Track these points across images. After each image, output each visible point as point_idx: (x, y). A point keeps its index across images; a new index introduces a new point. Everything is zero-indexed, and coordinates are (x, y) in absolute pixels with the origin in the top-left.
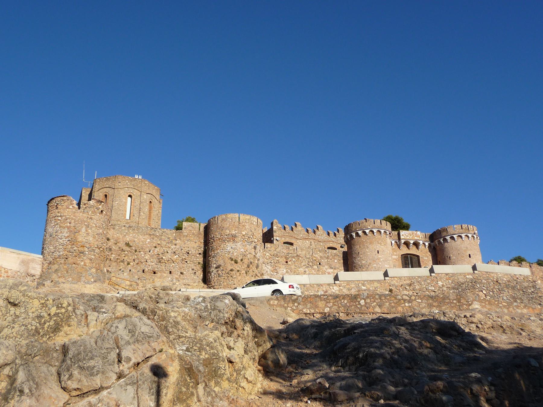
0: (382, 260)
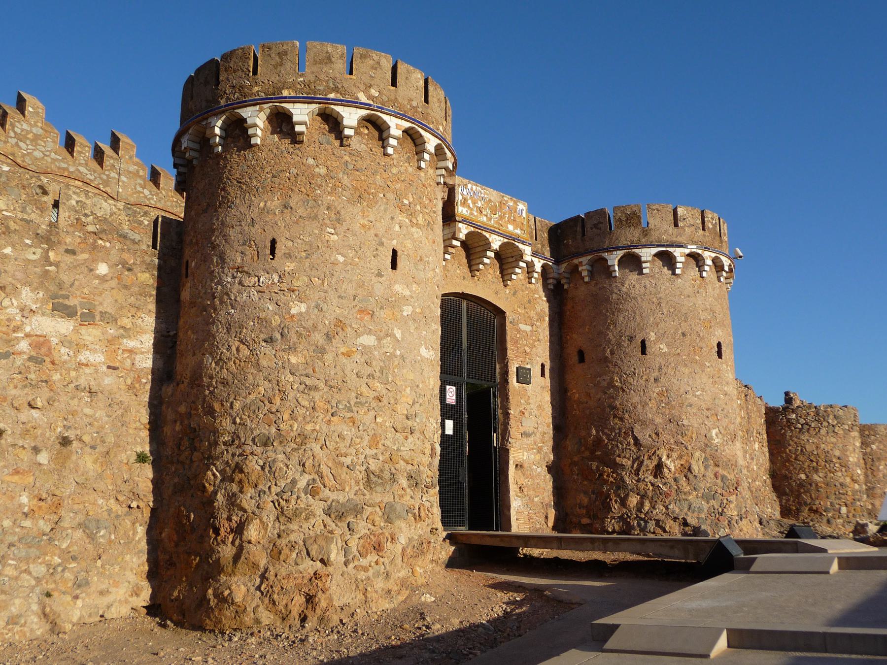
0: (407, 310)
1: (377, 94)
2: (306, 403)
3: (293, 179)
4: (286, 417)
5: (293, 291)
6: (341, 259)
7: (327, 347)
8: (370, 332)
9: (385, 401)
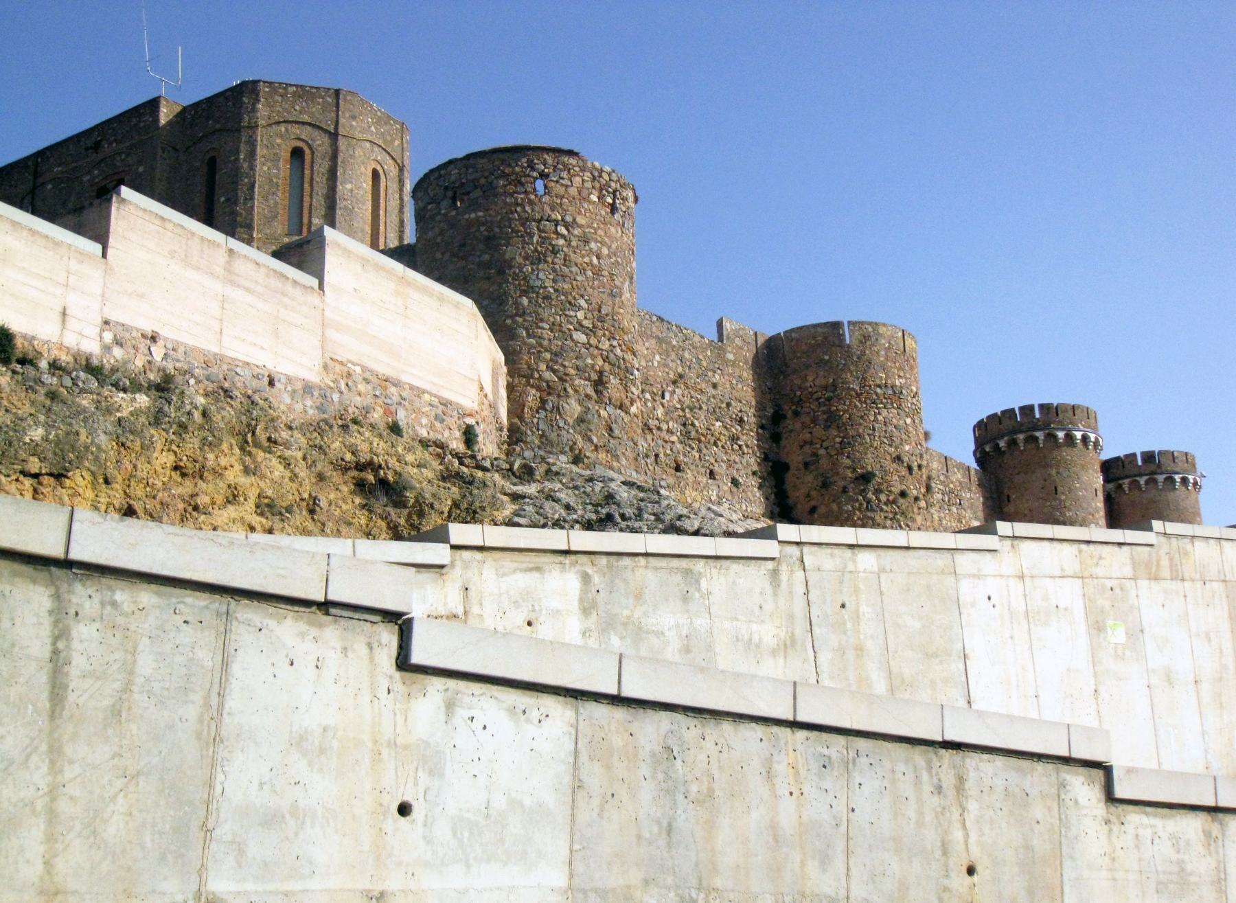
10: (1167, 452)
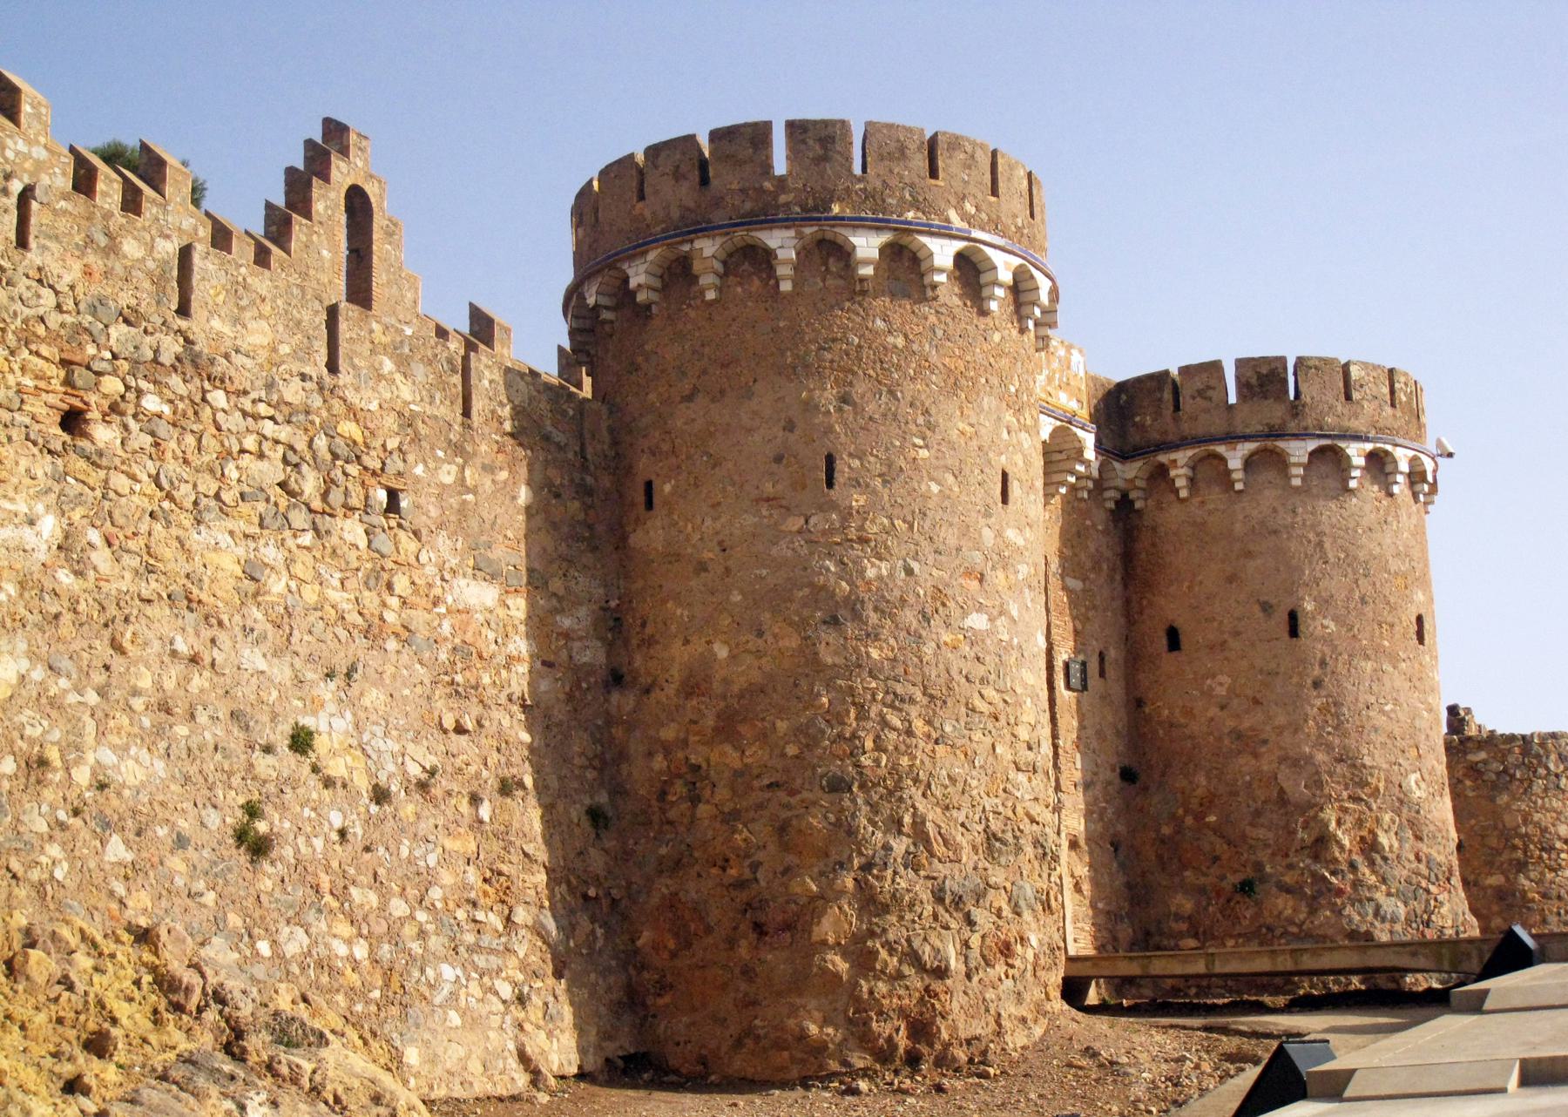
1: (973, 211)
2: (898, 724)
3: (853, 354)
4: (869, 744)
5: (867, 541)
6: (935, 488)
7: (924, 633)
8: (980, 608)
9: (1003, 722)
10: (1326, 361)
